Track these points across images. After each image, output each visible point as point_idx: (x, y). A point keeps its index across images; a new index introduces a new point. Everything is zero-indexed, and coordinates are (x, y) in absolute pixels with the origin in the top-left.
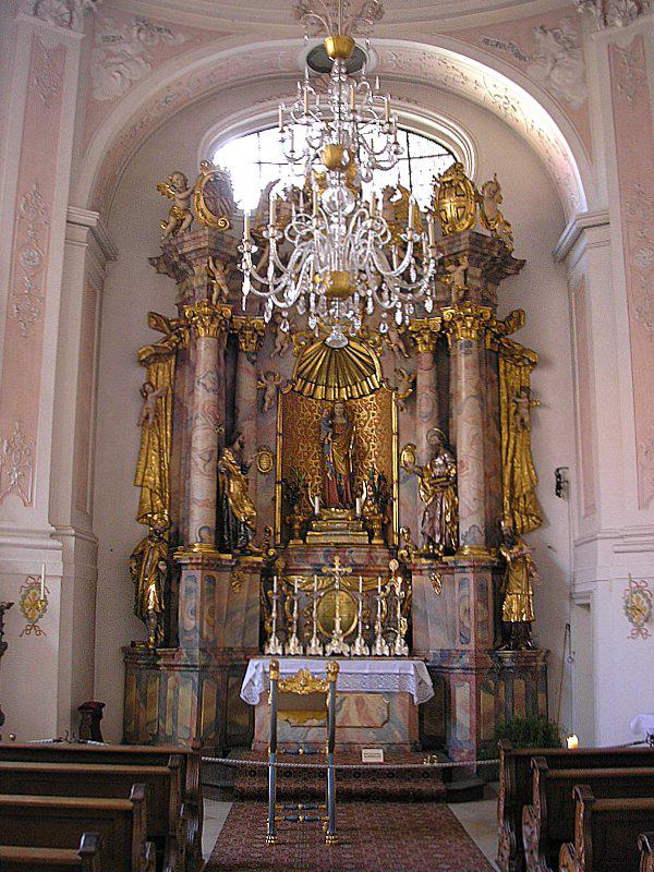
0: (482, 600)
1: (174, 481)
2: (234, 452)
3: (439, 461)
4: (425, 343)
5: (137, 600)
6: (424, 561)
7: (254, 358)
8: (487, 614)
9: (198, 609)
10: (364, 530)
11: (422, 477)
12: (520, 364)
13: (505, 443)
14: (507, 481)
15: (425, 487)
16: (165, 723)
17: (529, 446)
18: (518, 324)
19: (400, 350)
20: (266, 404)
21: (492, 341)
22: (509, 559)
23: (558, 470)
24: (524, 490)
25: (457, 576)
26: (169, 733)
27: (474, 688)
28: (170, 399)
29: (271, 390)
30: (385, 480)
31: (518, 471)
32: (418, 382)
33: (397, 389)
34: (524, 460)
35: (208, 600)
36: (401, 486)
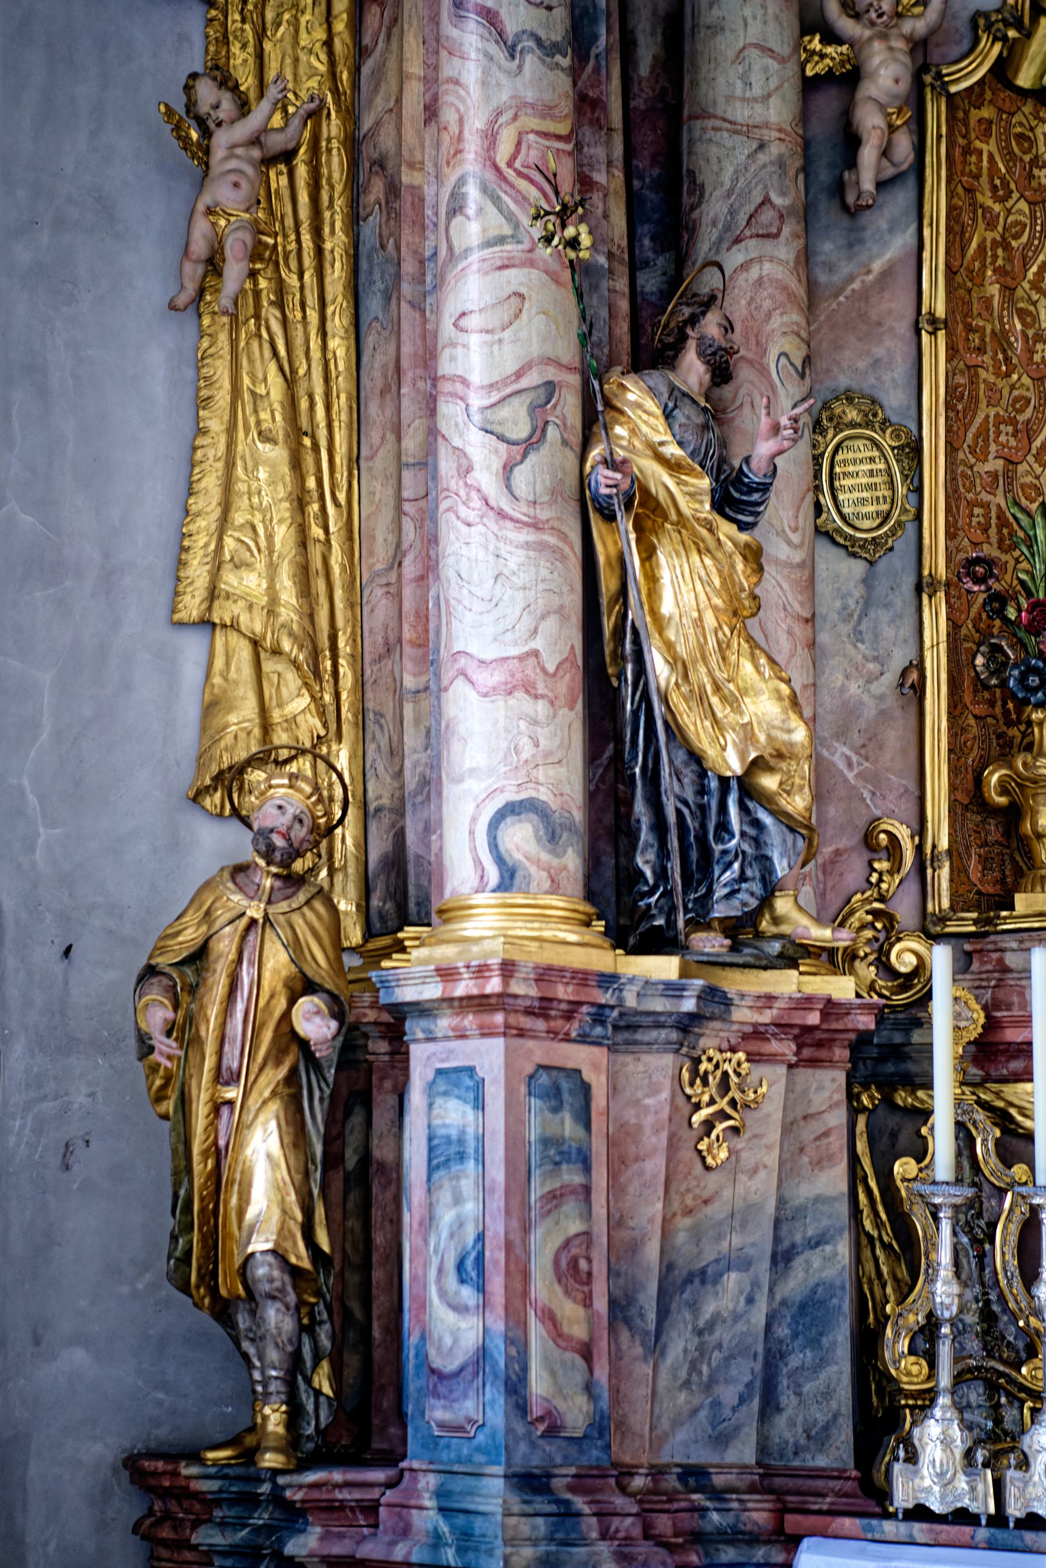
1: (378, 600)
5: (182, 1207)
9: (495, 1255)
20: (868, 155)
28: (335, 166)
35: (554, 1198)
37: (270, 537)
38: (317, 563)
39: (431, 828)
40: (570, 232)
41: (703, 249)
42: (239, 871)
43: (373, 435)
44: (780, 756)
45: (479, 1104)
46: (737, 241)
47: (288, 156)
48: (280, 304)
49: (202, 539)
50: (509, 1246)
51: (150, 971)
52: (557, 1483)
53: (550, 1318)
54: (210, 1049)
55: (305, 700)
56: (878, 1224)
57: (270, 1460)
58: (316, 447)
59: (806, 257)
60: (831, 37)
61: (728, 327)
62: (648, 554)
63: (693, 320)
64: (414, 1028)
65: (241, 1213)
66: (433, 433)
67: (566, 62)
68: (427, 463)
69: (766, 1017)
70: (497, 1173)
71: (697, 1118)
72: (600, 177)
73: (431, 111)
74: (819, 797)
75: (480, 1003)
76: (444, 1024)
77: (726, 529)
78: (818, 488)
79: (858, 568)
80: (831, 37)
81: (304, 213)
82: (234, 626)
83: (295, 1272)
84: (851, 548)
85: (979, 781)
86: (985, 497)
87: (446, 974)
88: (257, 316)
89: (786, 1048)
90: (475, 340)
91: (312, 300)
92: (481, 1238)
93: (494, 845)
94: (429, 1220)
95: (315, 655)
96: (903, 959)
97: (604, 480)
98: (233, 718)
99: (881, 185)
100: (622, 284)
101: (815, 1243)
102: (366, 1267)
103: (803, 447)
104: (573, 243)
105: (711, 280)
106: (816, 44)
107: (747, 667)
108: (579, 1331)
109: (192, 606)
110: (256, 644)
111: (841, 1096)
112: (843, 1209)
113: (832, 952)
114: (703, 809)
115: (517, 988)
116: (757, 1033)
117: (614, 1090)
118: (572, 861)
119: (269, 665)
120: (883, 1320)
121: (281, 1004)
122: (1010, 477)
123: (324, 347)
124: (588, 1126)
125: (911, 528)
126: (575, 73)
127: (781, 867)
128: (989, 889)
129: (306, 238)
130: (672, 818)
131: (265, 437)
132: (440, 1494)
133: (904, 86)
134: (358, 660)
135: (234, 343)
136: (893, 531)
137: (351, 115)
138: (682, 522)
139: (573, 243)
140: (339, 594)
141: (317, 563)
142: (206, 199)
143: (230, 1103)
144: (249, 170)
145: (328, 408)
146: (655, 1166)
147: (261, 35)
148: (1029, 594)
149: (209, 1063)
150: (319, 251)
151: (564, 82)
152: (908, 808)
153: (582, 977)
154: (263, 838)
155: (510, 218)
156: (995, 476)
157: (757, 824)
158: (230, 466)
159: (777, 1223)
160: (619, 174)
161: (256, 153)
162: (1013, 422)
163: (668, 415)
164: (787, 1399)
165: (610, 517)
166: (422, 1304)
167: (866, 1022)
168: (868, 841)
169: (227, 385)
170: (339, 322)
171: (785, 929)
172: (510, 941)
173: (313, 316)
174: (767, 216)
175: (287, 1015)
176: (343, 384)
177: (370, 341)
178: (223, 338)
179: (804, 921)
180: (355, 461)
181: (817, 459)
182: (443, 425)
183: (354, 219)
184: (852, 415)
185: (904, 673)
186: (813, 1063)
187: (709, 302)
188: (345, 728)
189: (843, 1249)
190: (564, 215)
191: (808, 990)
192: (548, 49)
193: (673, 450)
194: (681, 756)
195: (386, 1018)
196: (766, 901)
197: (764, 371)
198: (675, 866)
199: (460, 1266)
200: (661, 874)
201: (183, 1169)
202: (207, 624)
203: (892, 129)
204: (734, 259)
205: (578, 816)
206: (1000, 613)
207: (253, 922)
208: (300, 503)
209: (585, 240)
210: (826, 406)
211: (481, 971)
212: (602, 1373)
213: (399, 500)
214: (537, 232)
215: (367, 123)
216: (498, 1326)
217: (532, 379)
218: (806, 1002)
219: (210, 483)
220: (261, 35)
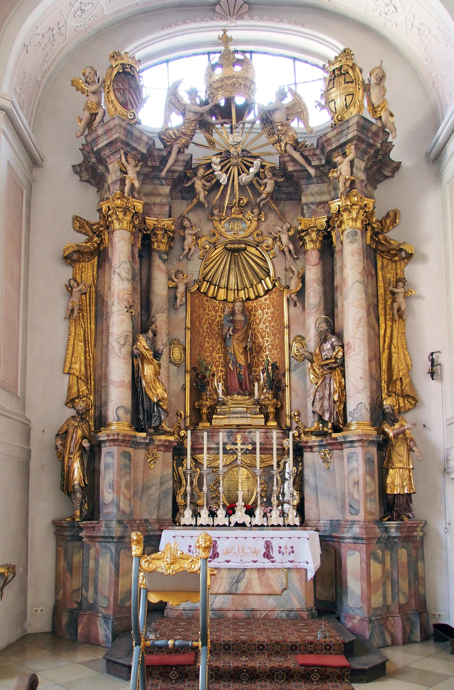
0: (369, 473)
1: (98, 369)
2: (147, 339)
3: (328, 346)
4: (312, 241)
5: (63, 476)
6: (314, 438)
7: (165, 257)
8: (374, 487)
9: (115, 483)
10: (261, 412)
11: (312, 361)
12: (397, 258)
13: (382, 332)
14: (384, 366)
15: (314, 371)
16: (87, 590)
17: (404, 333)
18: (394, 222)
19: (290, 251)
20: (178, 300)
21: (372, 238)
22: (391, 435)
23: (432, 354)
24: (401, 374)
25: (346, 451)
26: (91, 601)
27: (364, 557)
28: (94, 295)
29: (181, 288)
30: (277, 369)
31: (395, 356)
32: (306, 278)
33: (288, 287)
34: (400, 347)
35: (125, 474)
36: (293, 374)
37: (80, 359)
38: (88, 363)
39: (106, 410)
40: (131, 310)
41: (153, 313)
42: (73, 417)
43: (99, 341)
44: (163, 399)
45: (113, 458)
46: (158, 313)
47: (85, 294)
48: (83, 318)
49: (69, 359)
50: (117, 482)
51: (58, 435)
52: (124, 522)
53: (124, 494)
54: (68, 448)
55: (85, 387)
56: (177, 478)
57: (78, 519)
58: (88, 343)
59: (168, 317)
60: (173, 281)
61: (156, 327)
62: (143, 365)
63: (151, 326)
64: (103, 445)
65: (73, 477)
66: (108, 342)
67: (131, 282)
68: (107, 347)
69: (160, 443)
70: (116, 470)
71: (149, 460)
72: (136, 301)
73: (109, 288)
74: (169, 406)
75: (114, 441)
76: (107, 444)
77: (155, 360)
78: (170, 354)
79: (176, 368)
80: (173, 281)
81: (88, 303)
82: (73, 374)
83: (82, 487)
84: (175, 364)
85: (194, 404)
86: (196, 357)
87: (108, 435)
88: (79, 320)
89: (163, 449)
90: (115, 327)
91: (89, 318)
92: (113, 481)
93: (116, 414)
94: (104, 478)
95: (87, 379)
96: (182, 433)
97: (136, 351)
98: (73, 390)
99: (180, 305)
100: (140, 319)
101: (167, 481)
102: (94, 487)
103: (168, 348)
104: (132, 312)
105: (153, 319)
106: (171, 282)
107: (158, 384)
108: (129, 497)
109: (67, 370)
110: (77, 377)
111: (172, 457)
112: (171, 476)
113: (171, 432)
114: (151, 408)
115: (120, 438)
116: (158, 446)
117: (135, 456)
118: (129, 416)
119: (79, 381)
120: (177, 494)
121: (81, 441)
122: (200, 355)
123: (90, 326)
124: (131, 461)
125: (184, 362)
126: (132, 284)
127: (163, 418)
128: (196, 422)
129: (88, 307)
130: (146, 409)
131: (80, 341)
132: (105, 524)
133: (184, 290)
134: (94, 381)
135: (75, 325)
136: (181, 362)
137: (96, 287)
138: (148, 359)
139: (132, 312)
140: (92, 369)
141: (88, 363)
142: (71, 300)
143: (71, 458)
144: (79, 296)
145: (91, 336)
146: (141, 469)
147: (82, 273)
148: (202, 373)
149: (68, 451)
150: (90, 310)
151: (131, 286)
152: (183, 409)
153: (130, 436)
154: (78, 411)
155: (122, 307)
156: (197, 354)
157: (159, 410)
158: (74, 346)
159: (161, 478)
160: (139, 301)
161: (80, 293)
162: (200, 345)
163: (146, 341)
164: (162, 508)
165: (136, 358)
166: (103, 492)
167: (175, 444)
168: (177, 414)
169: (74, 331)
170: (93, 322)
171: (163, 428)
172: (119, 430)
173: (89, 321)
174: (163, 309)
175: (81, 442)
176: (93, 332)
177: (98, 325)
178: (73, 324)
179: (166, 427)
180: (95, 346)
181: (170, 349)
182: (110, 341)
183: (96, 305)
184: (176, 343)
185: (183, 386)
186: (167, 451)
187: (153, 323)
188: (92, 393)
189: (171, 483)
190: (130, 307)
191: (167, 439)
192: (128, 280)
193: (147, 347)
194: (147, 399)
195: (98, 443)
196: (160, 424)
197: (162, 334)
198: (146, 417)
199: (109, 486)
200: (144, 419)
201: (63, 470)
202: (69, 373)
203: (182, 297)
204: (157, 316)
205: (130, 408)
206: (198, 376)
207: (76, 426)
208: (85, 352)
209: (134, 312)
210: (172, 341)
211: (114, 435)
212: (132, 504)
213: (102, 353)
214: (126, 310)
215: (99, 289)
216: (115, 496)
217: (125, 334)
218: (166, 441)
219: (70, 349)
220: (82, 273)
